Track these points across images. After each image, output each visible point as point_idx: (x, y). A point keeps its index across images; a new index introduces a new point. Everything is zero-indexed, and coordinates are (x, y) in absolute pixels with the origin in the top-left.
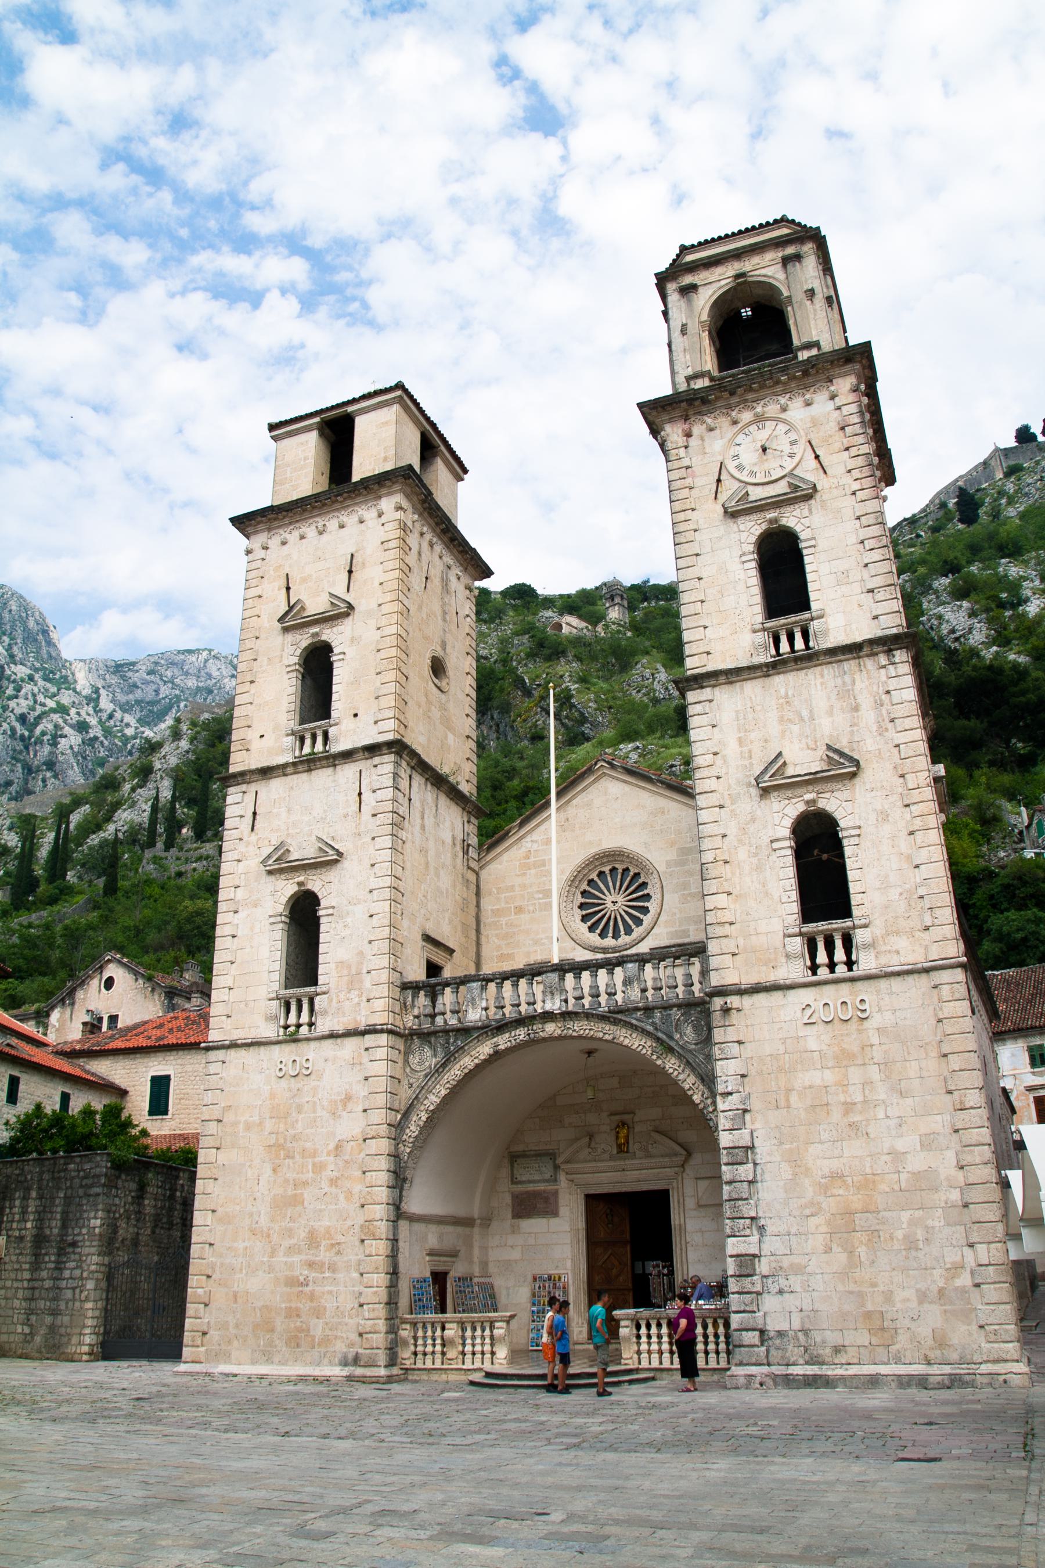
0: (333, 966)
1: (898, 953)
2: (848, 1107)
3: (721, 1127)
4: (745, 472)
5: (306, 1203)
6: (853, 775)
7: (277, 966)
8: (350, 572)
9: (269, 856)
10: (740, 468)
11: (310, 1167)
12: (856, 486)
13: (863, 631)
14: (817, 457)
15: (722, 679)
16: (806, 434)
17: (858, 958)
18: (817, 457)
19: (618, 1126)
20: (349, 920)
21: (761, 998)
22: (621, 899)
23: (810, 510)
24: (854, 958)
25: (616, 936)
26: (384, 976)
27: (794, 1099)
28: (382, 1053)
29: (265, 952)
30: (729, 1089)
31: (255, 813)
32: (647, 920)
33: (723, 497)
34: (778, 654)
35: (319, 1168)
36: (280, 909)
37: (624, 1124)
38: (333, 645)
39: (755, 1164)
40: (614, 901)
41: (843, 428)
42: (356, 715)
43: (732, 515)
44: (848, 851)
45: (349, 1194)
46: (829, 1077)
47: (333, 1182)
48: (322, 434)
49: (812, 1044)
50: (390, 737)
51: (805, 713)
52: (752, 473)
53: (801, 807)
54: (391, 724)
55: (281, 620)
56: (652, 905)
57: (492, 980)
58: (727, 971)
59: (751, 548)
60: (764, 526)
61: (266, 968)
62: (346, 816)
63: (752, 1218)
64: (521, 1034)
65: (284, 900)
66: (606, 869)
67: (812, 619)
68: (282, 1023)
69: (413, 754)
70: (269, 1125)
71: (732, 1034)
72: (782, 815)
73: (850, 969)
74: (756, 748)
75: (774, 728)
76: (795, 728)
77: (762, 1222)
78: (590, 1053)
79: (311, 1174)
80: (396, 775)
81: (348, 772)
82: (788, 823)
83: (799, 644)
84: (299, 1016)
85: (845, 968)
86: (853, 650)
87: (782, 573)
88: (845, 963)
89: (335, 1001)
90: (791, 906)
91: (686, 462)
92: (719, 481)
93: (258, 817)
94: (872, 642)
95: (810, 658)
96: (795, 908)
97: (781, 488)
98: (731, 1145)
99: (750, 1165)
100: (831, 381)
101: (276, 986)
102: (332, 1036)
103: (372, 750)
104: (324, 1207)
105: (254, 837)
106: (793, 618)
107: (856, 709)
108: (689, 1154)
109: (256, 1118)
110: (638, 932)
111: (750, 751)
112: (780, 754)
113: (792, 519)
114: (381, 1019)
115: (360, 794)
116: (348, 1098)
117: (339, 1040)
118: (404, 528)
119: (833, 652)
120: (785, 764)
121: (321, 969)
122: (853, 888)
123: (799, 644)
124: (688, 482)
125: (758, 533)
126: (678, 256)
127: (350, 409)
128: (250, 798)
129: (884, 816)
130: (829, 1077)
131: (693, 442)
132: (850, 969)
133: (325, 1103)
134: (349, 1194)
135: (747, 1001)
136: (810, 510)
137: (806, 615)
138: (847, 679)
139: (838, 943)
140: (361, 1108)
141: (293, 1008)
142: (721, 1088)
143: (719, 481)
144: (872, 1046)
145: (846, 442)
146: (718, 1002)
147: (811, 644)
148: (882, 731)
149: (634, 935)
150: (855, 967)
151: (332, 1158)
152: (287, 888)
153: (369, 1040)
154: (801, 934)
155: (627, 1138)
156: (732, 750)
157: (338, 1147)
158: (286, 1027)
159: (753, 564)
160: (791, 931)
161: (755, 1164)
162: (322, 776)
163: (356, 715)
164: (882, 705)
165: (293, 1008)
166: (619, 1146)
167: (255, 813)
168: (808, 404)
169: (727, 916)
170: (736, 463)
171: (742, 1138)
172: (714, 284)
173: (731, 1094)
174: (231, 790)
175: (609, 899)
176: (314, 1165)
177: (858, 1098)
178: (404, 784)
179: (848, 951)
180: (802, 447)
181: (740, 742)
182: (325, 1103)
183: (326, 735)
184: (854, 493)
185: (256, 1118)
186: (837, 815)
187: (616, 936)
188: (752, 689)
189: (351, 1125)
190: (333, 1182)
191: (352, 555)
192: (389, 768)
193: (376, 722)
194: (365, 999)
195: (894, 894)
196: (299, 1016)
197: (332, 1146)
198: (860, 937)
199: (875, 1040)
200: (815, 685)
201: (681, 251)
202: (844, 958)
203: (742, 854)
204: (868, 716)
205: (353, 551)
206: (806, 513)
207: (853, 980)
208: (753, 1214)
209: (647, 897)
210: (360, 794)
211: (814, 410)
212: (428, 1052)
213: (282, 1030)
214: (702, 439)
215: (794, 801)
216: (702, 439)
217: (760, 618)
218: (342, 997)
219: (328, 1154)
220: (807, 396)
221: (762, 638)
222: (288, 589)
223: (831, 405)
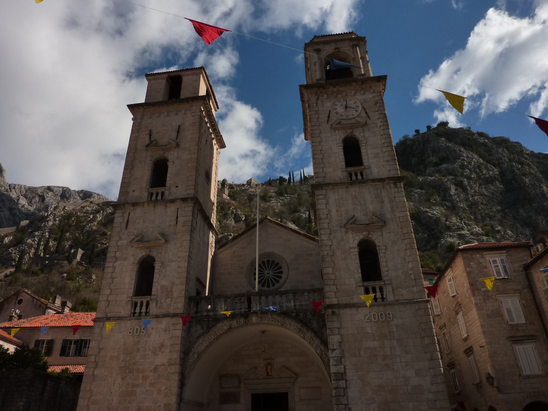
0: (159, 287)
1: (402, 295)
2: (385, 357)
3: (331, 364)
4: (339, 115)
5: (137, 395)
6: (382, 226)
7: (132, 286)
8: (178, 132)
9: (133, 239)
10: (337, 113)
11: (141, 377)
12: (381, 124)
13: (384, 174)
14: (366, 112)
15: (330, 186)
16: (362, 104)
17: (386, 296)
18: (366, 112)
19: (267, 364)
20: (168, 268)
21: (347, 311)
22: (271, 273)
23: (364, 131)
24: (384, 296)
25: (268, 286)
26: (183, 293)
27: (362, 353)
28: (180, 326)
29: (127, 280)
30: (335, 347)
31: (128, 221)
32: (281, 281)
33: (330, 123)
34: (351, 180)
35: (145, 378)
36: (137, 262)
37: (269, 364)
38: (169, 159)
39: (346, 381)
40: (269, 273)
41: (376, 104)
42: (177, 187)
43: (335, 129)
44: (381, 255)
45: (159, 391)
46: (376, 344)
47: (152, 385)
48: (167, 80)
49: (369, 330)
50: (192, 196)
51: (362, 202)
52: (341, 115)
53: (362, 237)
54: (192, 191)
55: (147, 146)
56: (284, 276)
57: (230, 298)
58: (331, 298)
59: (341, 141)
60: (346, 135)
61: (127, 287)
62: (170, 226)
63: (345, 405)
64: (242, 320)
65: (138, 259)
66: (265, 260)
67: (365, 169)
68: (132, 311)
69: (200, 205)
70: (122, 357)
71: (336, 325)
72: (353, 240)
73: (383, 301)
76: (359, 207)
77: (350, 406)
78: (263, 332)
79: (141, 381)
80: (193, 212)
81: (172, 209)
82: (356, 242)
83: (359, 177)
84: (141, 309)
85: (381, 300)
86: (382, 180)
87: (352, 152)
88: (381, 298)
89: (159, 302)
90: (358, 275)
91: (316, 109)
92: (329, 117)
93: (129, 224)
94: (389, 178)
95: (364, 181)
96: (360, 275)
97: (353, 121)
98: (336, 372)
99: (344, 381)
100: (371, 88)
101: (131, 295)
102: (157, 317)
103: (184, 200)
104: (146, 396)
105: (126, 232)
106: (357, 168)
107: (383, 202)
108: (297, 378)
109: (116, 354)
110: (277, 285)
111: (341, 214)
112: (354, 216)
113: (358, 134)
114: (180, 311)
115: (177, 217)
116: (162, 346)
117: (160, 319)
119: (374, 180)
120: (355, 220)
121: (154, 289)
123: (359, 177)
124: (317, 116)
125: (343, 137)
126: (313, 39)
127: (181, 73)
128: (126, 215)
130: (376, 344)
131: (320, 103)
132: (383, 301)
133: (151, 348)
134: (159, 391)
135: (342, 312)
136: (364, 131)
137: (362, 167)
138: (379, 191)
139: (378, 290)
140: (168, 350)
141: (139, 305)
142: (330, 347)
143: (329, 117)
144: (393, 332)
145: (376, 109)
146: (330, 311)
147: (364, 178)
148: (393, 211)
149: (276, 286)
150: (385, 300)
151: (152, 374)
152: (141, 254)
153: (174, 320)
154: (363, 286)
155: (271, 369)
156: (334, 213)
157: (156, 369)
158: (134, 313)
159: (342, 148)
160: (359, 284)
161: (346, 381)
162: (160, 209)
163: (177, 187)
164: (393, 202)
165: (139, 305)
166: (268, 373)
167: (128, 221)
168: (364, 94)
169: (333, 277)
170: (335, 111)
171: (341, 369)
173: (335, 350)
174: (118, 211)
175: (266, 272)
176: (143, 376)
177: (389, 353)
178: (195, 216)
179: (382, 295)
180: (360, 109)
181: (337, 211)
182: (151, 348)
183: (163, 194)
184: (380, 127)
185: (116, 354)
186: (376, 241)
187: (268, 286)
188: (342, 192)
189: (162, 359)
190: (152, 385)
191: (179, 126)
192: (190, 209)
193: (186, 190)
194: (173, 302)
196: (141, 309)
197: (152, 367)
199: (395, 330)
201: (314, 38)
202: (381, 296)
203: (338, 253)
204: (387, 205)
205: (179, 124)
206: (362, 132)
207: (385, 305)
208: (346, 402)
209: (282, 272)
210: (177, 217)
212: (199, 327)
213: (132, 315)
214: (322, 101)
215: (359, 234)
216: (322, 101)
217: (344, 167)
218: (163, 301)
219: (151, 371)
220: (362, 92)
221: (345, 174)
222: (150, 135)
223: (371, 96)
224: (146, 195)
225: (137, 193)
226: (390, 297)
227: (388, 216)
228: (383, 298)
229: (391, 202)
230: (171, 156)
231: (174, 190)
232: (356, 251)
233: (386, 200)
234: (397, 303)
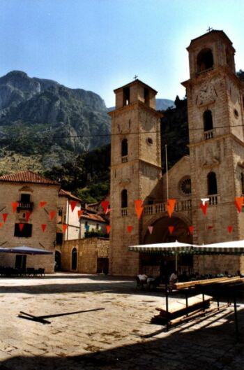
74: (202, 159)
75: (205, 155)
107: (220, 150)
118: (139, 113)
122: (218, 188)
129: (224, 173)
148: (225, 155)
152: (122, 189)
172: (199, 49)
181: (199, 158)
195: (225, 189)
198: (219, 198)
200: (212, 145)
203: (198, 181)
204: (222, 151)
211: (216, 81)
224: (120, 160)
225: (117, 160)
226: (219, 202)
227: (222, 158)
228: (217, 203)
229: (225, 149)
230: (127, 137)
231: (130, 156)
232: (206, 179)
233: (222, 148)
234: (224, 204)
